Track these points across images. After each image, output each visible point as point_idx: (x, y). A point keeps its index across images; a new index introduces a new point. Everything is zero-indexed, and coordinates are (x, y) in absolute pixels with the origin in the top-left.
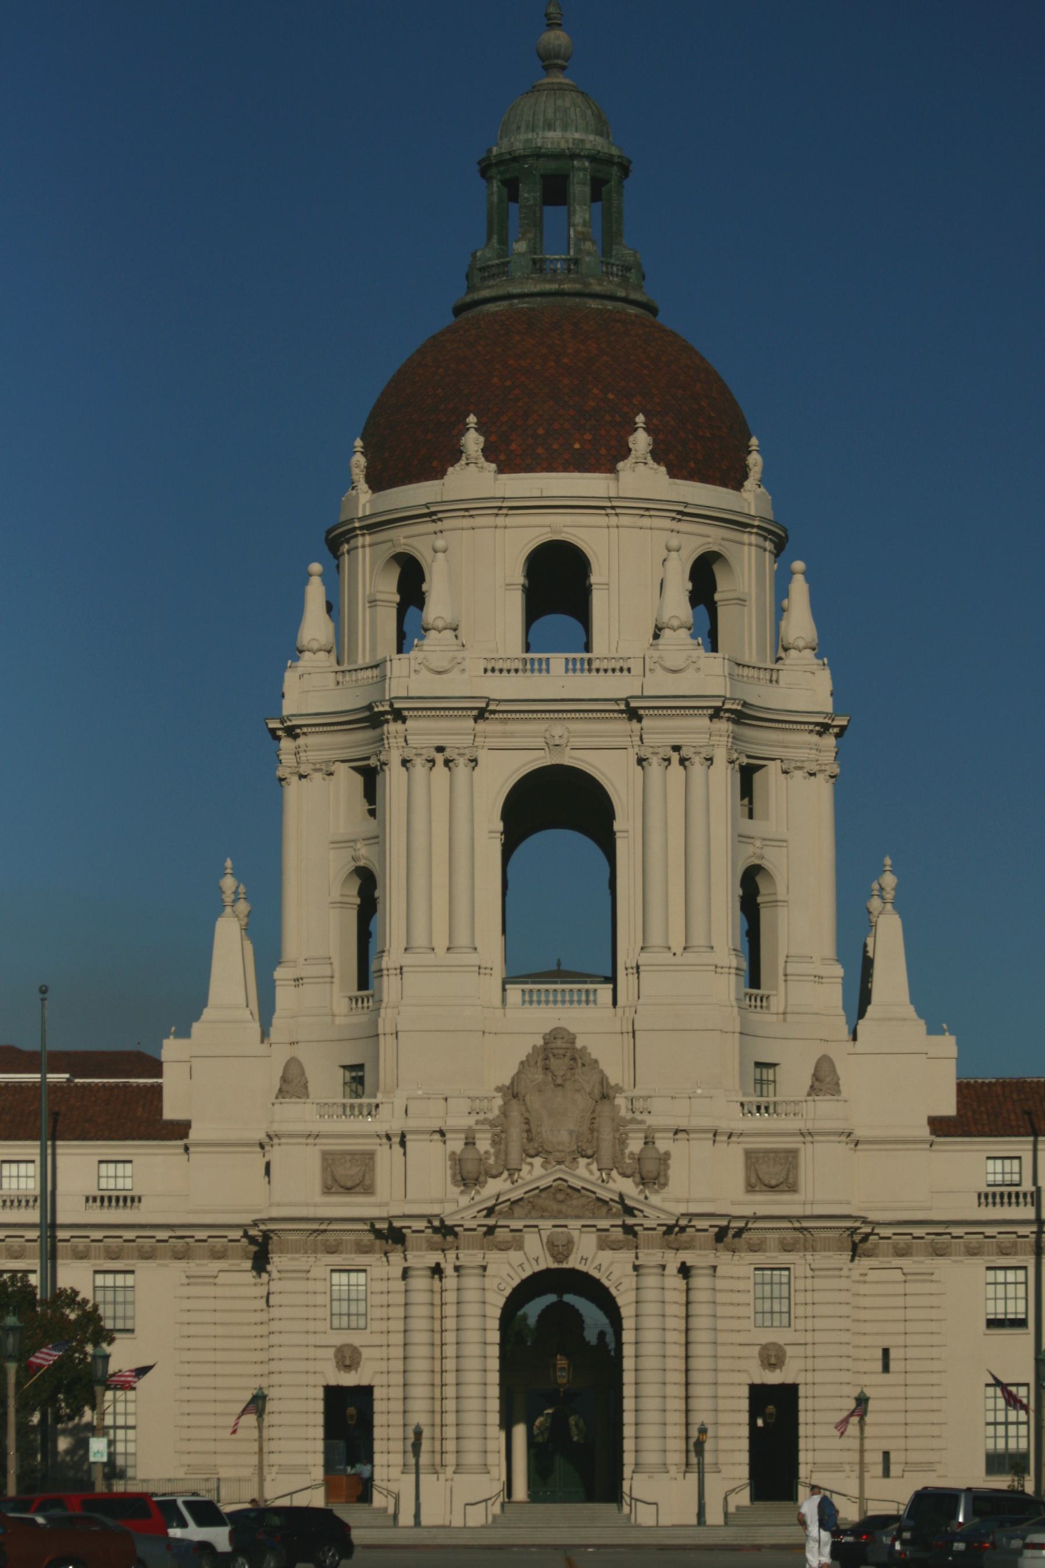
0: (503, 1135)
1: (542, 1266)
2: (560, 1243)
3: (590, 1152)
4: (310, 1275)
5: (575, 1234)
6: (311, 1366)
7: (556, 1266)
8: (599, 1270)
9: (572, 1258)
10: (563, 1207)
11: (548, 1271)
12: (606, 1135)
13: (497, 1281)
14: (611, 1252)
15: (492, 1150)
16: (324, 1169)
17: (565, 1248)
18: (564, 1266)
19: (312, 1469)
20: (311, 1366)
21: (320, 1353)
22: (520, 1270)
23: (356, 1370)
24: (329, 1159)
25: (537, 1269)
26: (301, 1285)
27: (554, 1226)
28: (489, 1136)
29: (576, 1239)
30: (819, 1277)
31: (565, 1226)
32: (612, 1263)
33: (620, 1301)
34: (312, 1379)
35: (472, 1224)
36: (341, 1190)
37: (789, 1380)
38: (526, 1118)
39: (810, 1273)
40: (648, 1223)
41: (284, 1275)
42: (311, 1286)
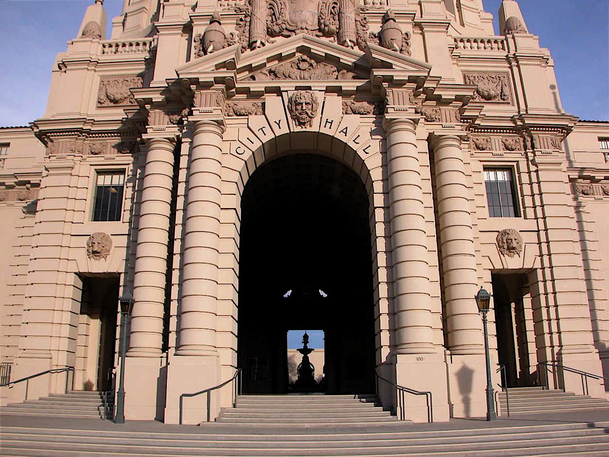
0: (248, 19)
1: (285, 130)
2: (303, 101)
3: (333, 28)
4: (74, 172)
5: (320, 96)
6: (64, 253)
7: (299, 129)
8: (346, 133)
9: (316, 121)
10: (306, 75)
11: (291, 134)
12: (350, 15)
13: (235, 145)
14: (359, 116)
15: (237, 33)
16: (100, 89)
17: (310, 107)
18: (308, 129)
19: (54, 354)
20: (64, 253)
21: (76, 241)
22: (260, 134)
23: (105, 258)
24: (104, 83)
25: (279, 133)
26: (65, 180)
27: (297, 88)
28: (235, 21)
29: (320, 101)
30: (542, 170)
31: (309, 88)
32: (359, 128)
33: (369, 164)
34: (63, 265)
35: (210, 78)
36: (112, 104)
37: (528, 266)
38: (270, 4)
39: (533, 168)
40: (398, 76)
41: (51, 172)
42: (74, 181)
